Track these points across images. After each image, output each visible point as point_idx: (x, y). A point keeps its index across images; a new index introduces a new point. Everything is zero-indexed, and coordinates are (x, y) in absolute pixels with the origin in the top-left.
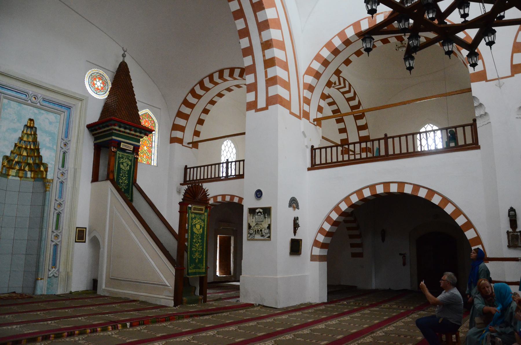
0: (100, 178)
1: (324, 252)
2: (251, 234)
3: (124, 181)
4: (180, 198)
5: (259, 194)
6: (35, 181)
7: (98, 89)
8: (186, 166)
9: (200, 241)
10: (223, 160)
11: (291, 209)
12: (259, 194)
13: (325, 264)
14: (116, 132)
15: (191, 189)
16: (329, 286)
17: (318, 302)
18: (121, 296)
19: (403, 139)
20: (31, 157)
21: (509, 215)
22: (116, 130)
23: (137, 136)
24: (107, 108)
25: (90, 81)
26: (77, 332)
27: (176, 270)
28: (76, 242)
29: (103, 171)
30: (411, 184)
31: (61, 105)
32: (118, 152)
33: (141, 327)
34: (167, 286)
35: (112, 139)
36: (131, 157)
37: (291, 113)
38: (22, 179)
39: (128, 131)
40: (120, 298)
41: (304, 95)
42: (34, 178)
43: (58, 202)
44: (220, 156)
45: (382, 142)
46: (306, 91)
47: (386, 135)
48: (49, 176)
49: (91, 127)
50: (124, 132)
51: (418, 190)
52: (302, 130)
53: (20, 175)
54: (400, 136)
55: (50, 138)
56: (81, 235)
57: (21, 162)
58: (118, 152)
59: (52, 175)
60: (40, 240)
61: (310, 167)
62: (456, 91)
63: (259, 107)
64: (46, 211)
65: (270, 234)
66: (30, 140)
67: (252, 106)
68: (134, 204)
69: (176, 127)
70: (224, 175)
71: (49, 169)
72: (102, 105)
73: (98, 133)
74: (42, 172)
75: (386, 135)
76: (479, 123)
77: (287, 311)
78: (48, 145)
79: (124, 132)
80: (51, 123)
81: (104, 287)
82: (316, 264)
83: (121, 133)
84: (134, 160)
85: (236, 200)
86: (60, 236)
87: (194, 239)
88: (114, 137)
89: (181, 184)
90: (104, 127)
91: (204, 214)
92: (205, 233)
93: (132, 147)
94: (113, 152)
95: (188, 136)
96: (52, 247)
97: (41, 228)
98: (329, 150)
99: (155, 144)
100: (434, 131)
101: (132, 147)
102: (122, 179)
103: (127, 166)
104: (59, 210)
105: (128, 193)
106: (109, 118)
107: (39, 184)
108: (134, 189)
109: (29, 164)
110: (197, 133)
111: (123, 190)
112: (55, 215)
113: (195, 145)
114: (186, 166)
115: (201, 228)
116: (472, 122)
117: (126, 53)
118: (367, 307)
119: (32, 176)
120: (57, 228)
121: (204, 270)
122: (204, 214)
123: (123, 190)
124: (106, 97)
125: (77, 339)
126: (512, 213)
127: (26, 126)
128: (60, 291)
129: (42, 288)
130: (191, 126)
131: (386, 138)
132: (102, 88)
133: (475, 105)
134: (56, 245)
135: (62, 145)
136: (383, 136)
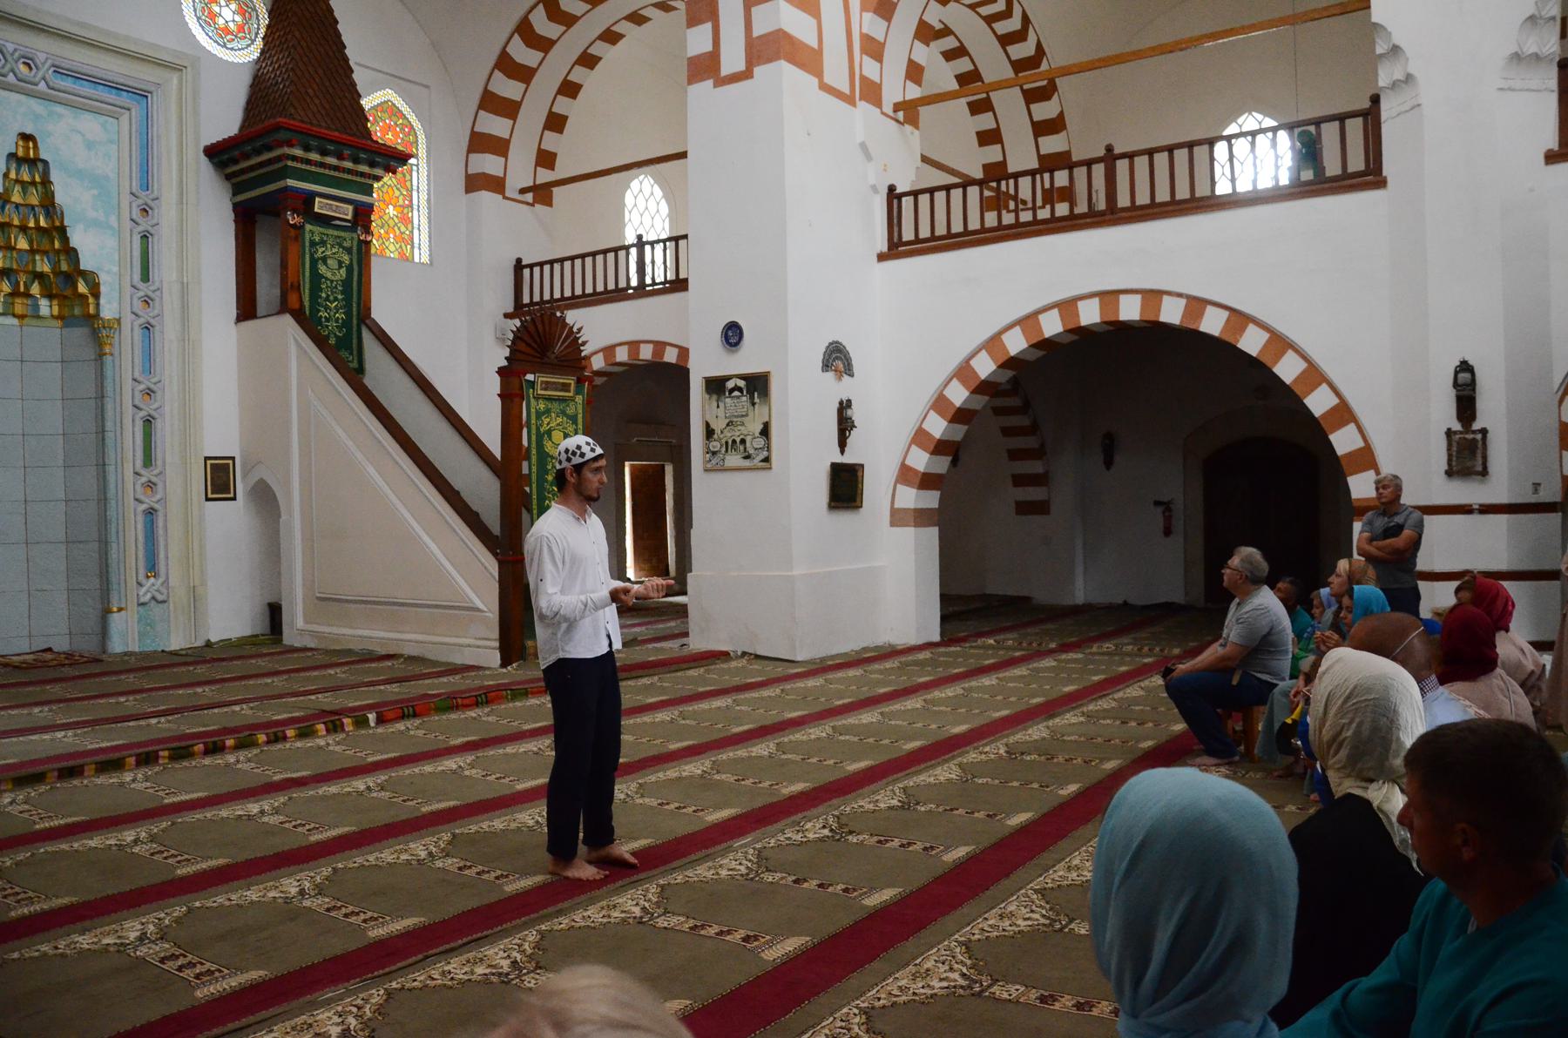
0: (260, 310)
1: (931, 499)
2: (714, 453)
3: (333, 314)
4: (499, 356)
5: (733, 335)
6: (65, 326)
7: (227, 31)
8: (519, 261)
10: (630, 239)
11: (830, 375)
12: (733, 335)
13: (934, 532)
14: (294, 164)
15: (532, 329)
16: (945, 598)
17: (913, 640)
18: (351, 647)
19: (1161, 159)
20: (45, 253)
21: (1456, 384)
22: (295, 155)
23: (362, 174)
24: (263, 94)
25: (199, 6)
26: (230, 742)
27: (501, 563)
28: (208, 499)
29: (267, 288)
30: (1180, 295)
31: (117, 88)
32: (308, 227)
33: (408, 723)
34: (478, 610)
35: (286, 188)
36: (349, 239)
37: (825, 88)
38: (26, 321)
39: (332, 160)
40: (349, 652)
41: (865, 31)
42: (60, 317)
43: (142, 387)
44: (621, 225)
45: (1099, 170)
46: (868, 16)
47: (1109, 149)
48: (108, 310)
49: (218, 154)
50: (323, 165)
51: (1200, 315)
52: (859, 140)
53: (19, 309)
54: (1150, 153)
55: (95, 192)
56: (220, 479)
57: (16, 272)
58: (308, 227)
59: (116, 305)
60: (103, 500)
61: (885, 249)
62: (1325, 9)
63: (726, 70)
64: (109, 414)
65: (769, 449)
66: (34, 200)
67: (705, 68)
68: (368, 381)
69: (480, 143)
70: (634, 283)
71: (102, 289)
72: (245, 80)
73: (243, 171)
74: (82, 296)
75: (1109, 149)
76: (1387, 109)
77: (821, 668)
78: (92, 214)
80: (90, 145)
81: (300, 623)
82: (908, 533)
83: (313, 169)
84: (359, 250)
85: (671, 356)
86: (160, 486)
88: (291, 182)
89: (507, 316)
90: (258, 152)
91: (572, 399)
93: (350, 208)
95: (520, 170)
96: (140, 518)
97: (102, 466)
98: (940, 197)
99: (420, 198)
100: (1253, 134)
101: (350, 208)
102: (327, 308)
103: (340, 267)
104: (149, 408)
105: (349, 349)
106: (272, 121)
107: (79, 334)
108: (368, 338)
109: (40, 276)
110: (546, 159)
111: (332, 341)
112: (139, 424)
113: (542, 194)
114: (519, 261)
116: (1366, 104)
118: (1051, 652)
119: (56, 311)
120: (148, 460)
122: (572, 399)
123: (332, 341)
124: (256, 55)
125: (231, 758)
126: (1464, 376)
128: (176, 642)
129: (125, 636)
130: (525, 135)
131: (1110, 158)
132: (241, 28)
133: (1379, 50)
134: (151, 513)
135: (136, 214)
136: (1102, 152)
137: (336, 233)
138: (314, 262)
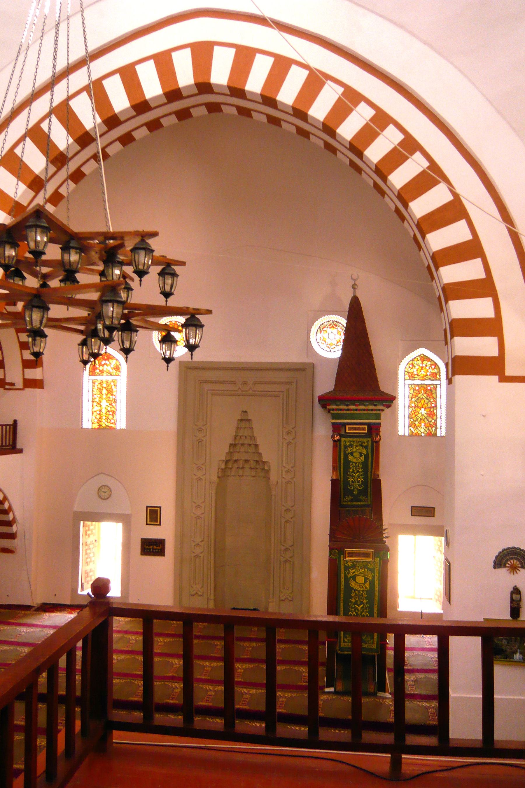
9: (365, 601)
23: (372, 410)
32: (343, 439)
36: (367, 441)
48: (274, 476)
50: (348, 410)
79: (348, 410)
87: (351, 597)
92: (376, 589)
93: (366, 426)
101: (366, 426)
102: (352, 476)
111: (356, 492)
115: (366, 582)
117: (356, 283)
121: (375, 646)
123: (356, 492)
127: (241, 420)
137: (359, 440)
138: (346, 456)
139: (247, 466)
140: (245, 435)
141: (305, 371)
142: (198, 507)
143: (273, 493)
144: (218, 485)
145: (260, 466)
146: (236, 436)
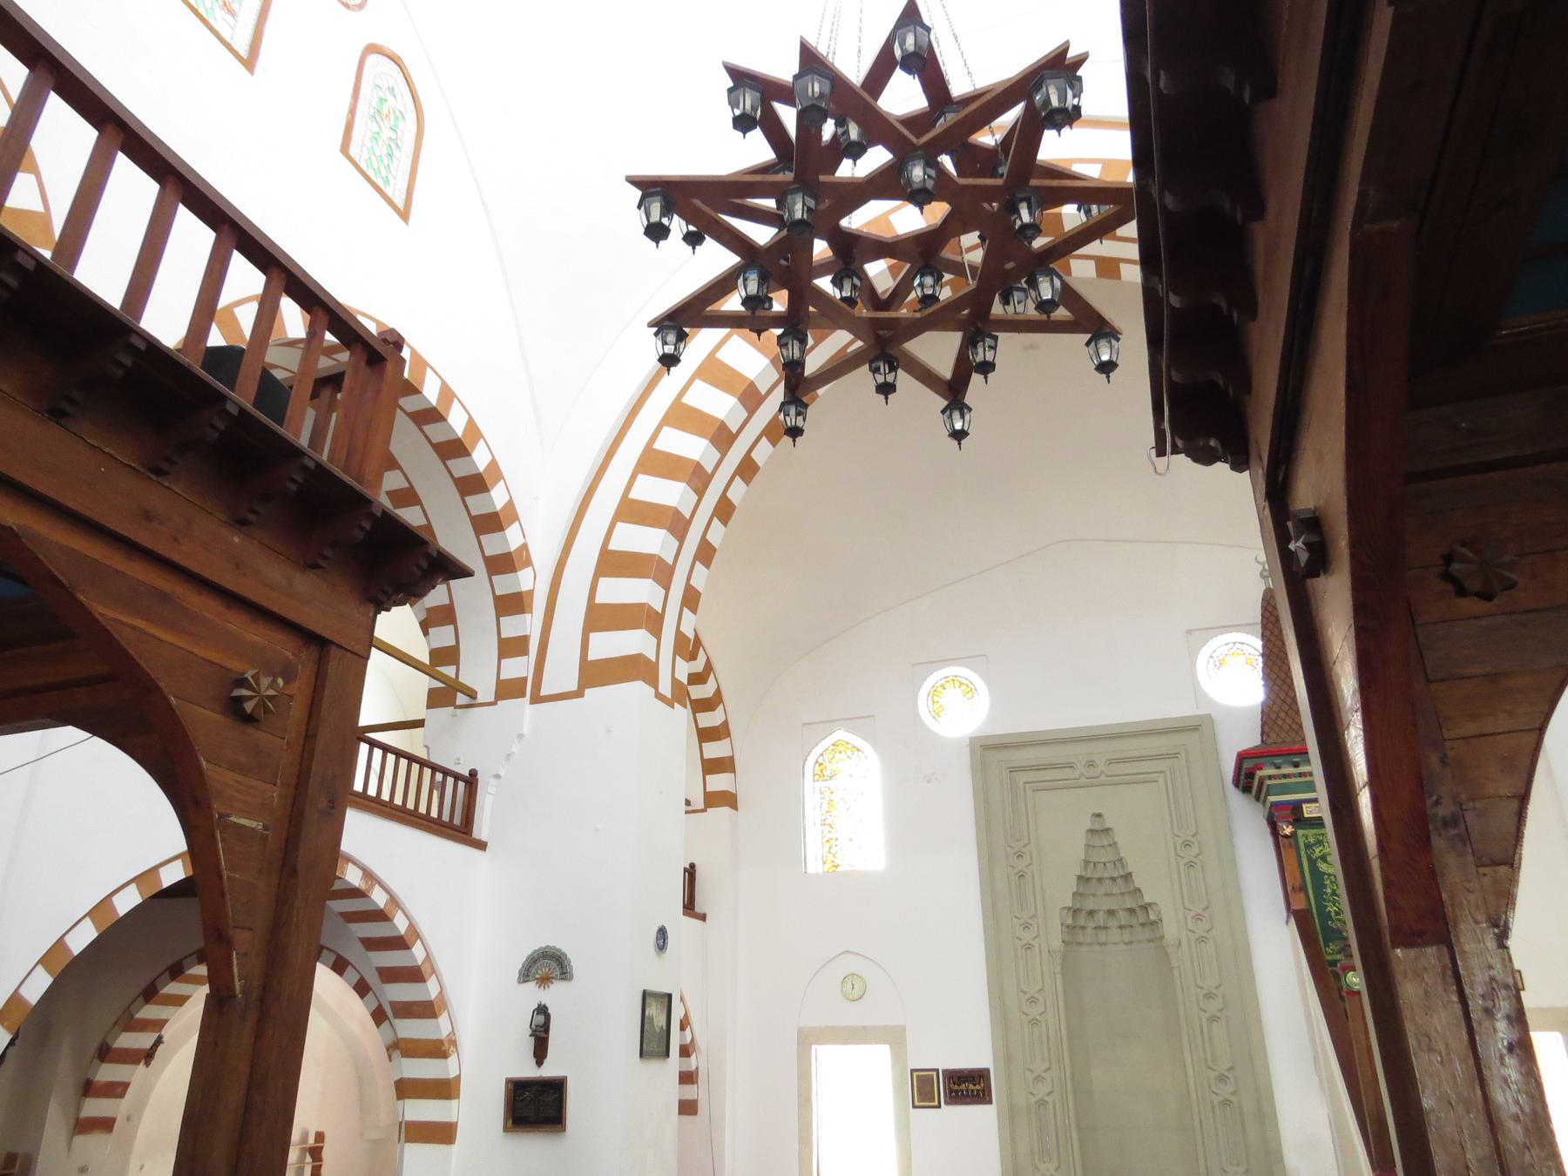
32: (1300, 832)
48: (1170, 930)
50: (1300, 775)
53: (1102, 939)
88: (1272, 799)
94: (1286, 836)
127: (1091, 831)
138: (1312, 863)
139: (1113, 923)
140: (1103, 860)
141: (1197, 728)
142: (1032, 1000)
143: (1174, 963)
144: (1064, 958)
145: (1143, 917)
146: (1087, 863)
